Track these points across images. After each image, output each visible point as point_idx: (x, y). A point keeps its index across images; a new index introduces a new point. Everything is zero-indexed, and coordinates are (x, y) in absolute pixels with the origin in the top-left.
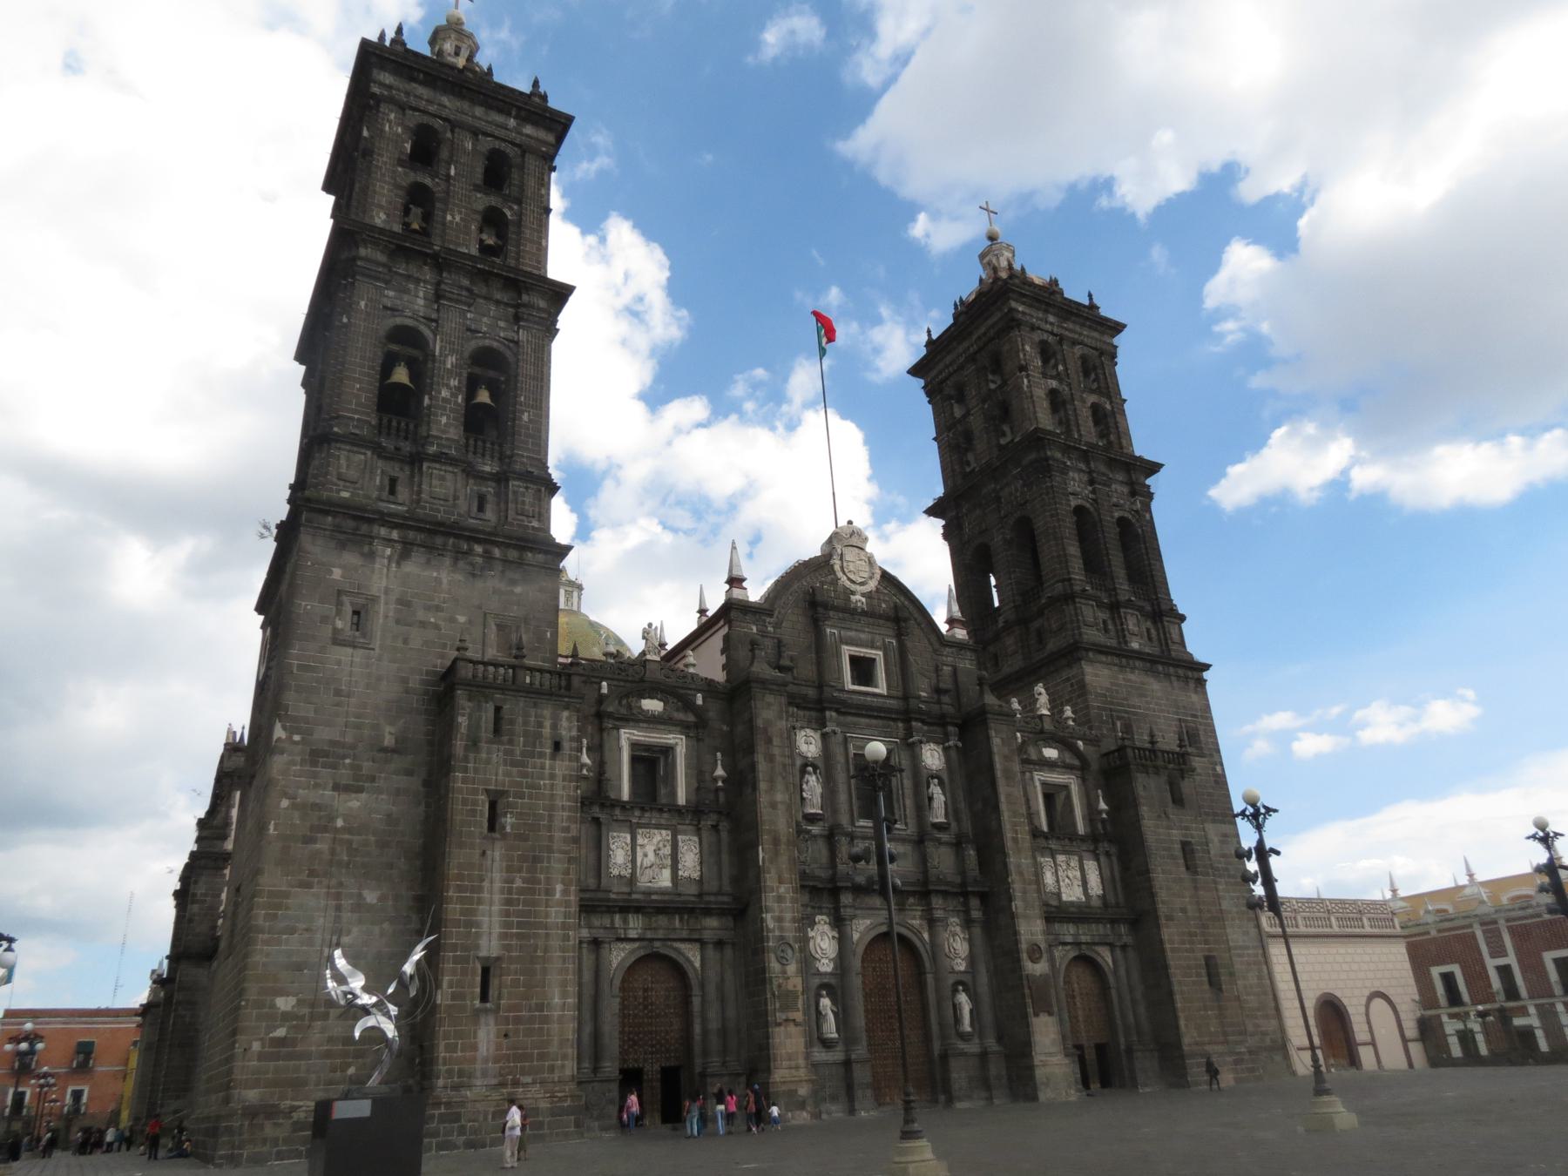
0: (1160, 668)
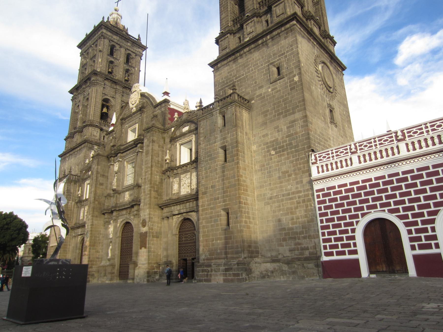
0: (260, 42)
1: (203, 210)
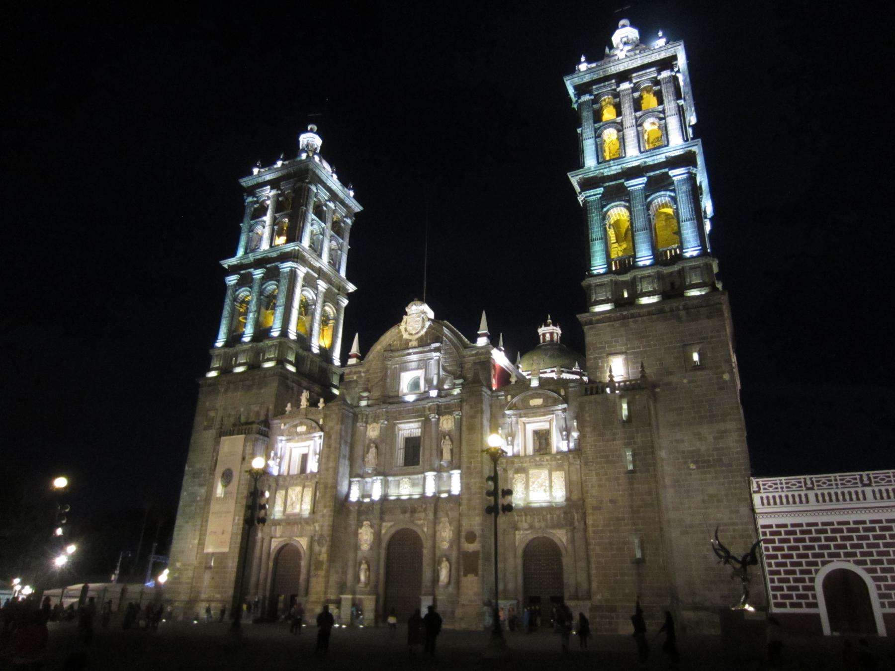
1: (594, 532)
